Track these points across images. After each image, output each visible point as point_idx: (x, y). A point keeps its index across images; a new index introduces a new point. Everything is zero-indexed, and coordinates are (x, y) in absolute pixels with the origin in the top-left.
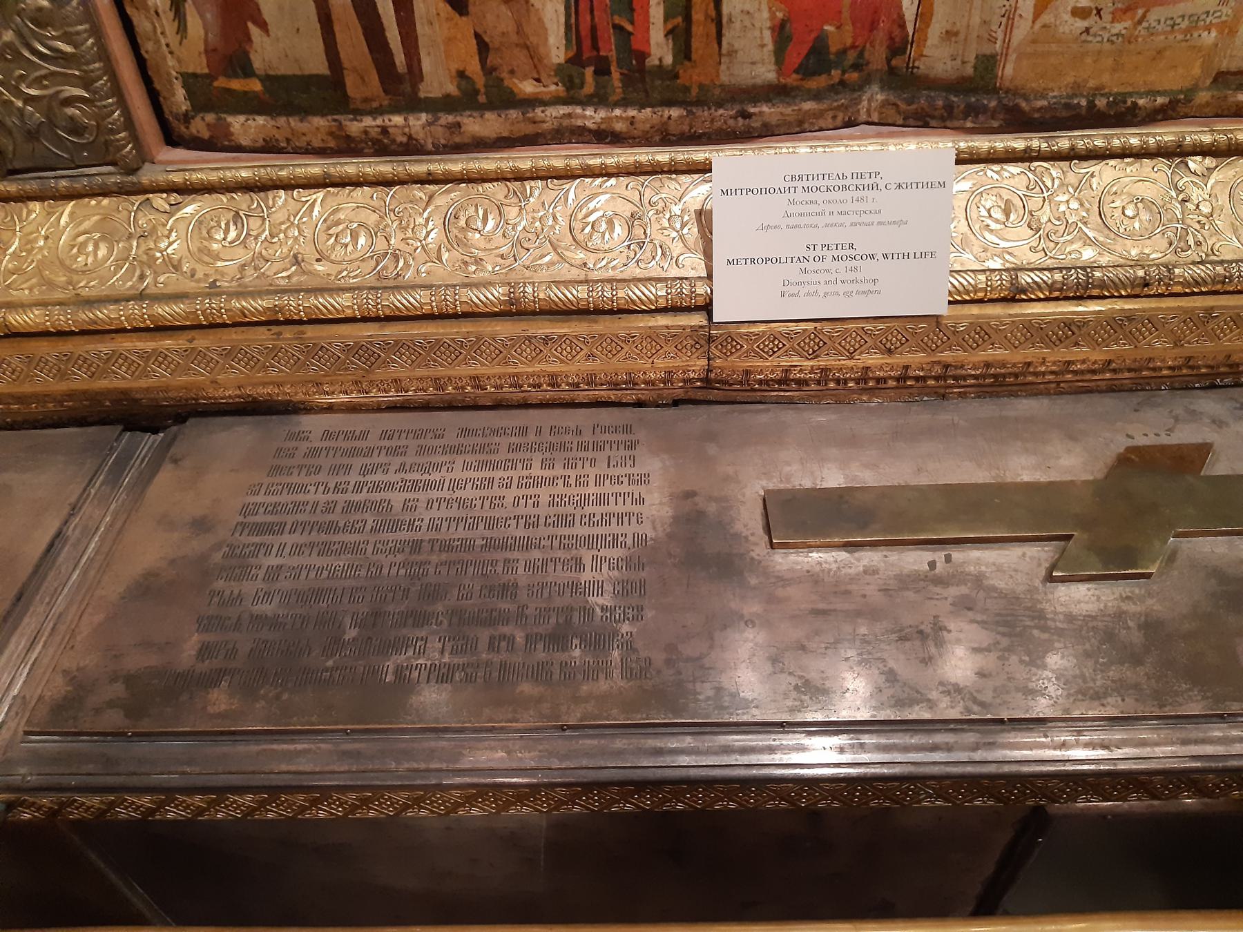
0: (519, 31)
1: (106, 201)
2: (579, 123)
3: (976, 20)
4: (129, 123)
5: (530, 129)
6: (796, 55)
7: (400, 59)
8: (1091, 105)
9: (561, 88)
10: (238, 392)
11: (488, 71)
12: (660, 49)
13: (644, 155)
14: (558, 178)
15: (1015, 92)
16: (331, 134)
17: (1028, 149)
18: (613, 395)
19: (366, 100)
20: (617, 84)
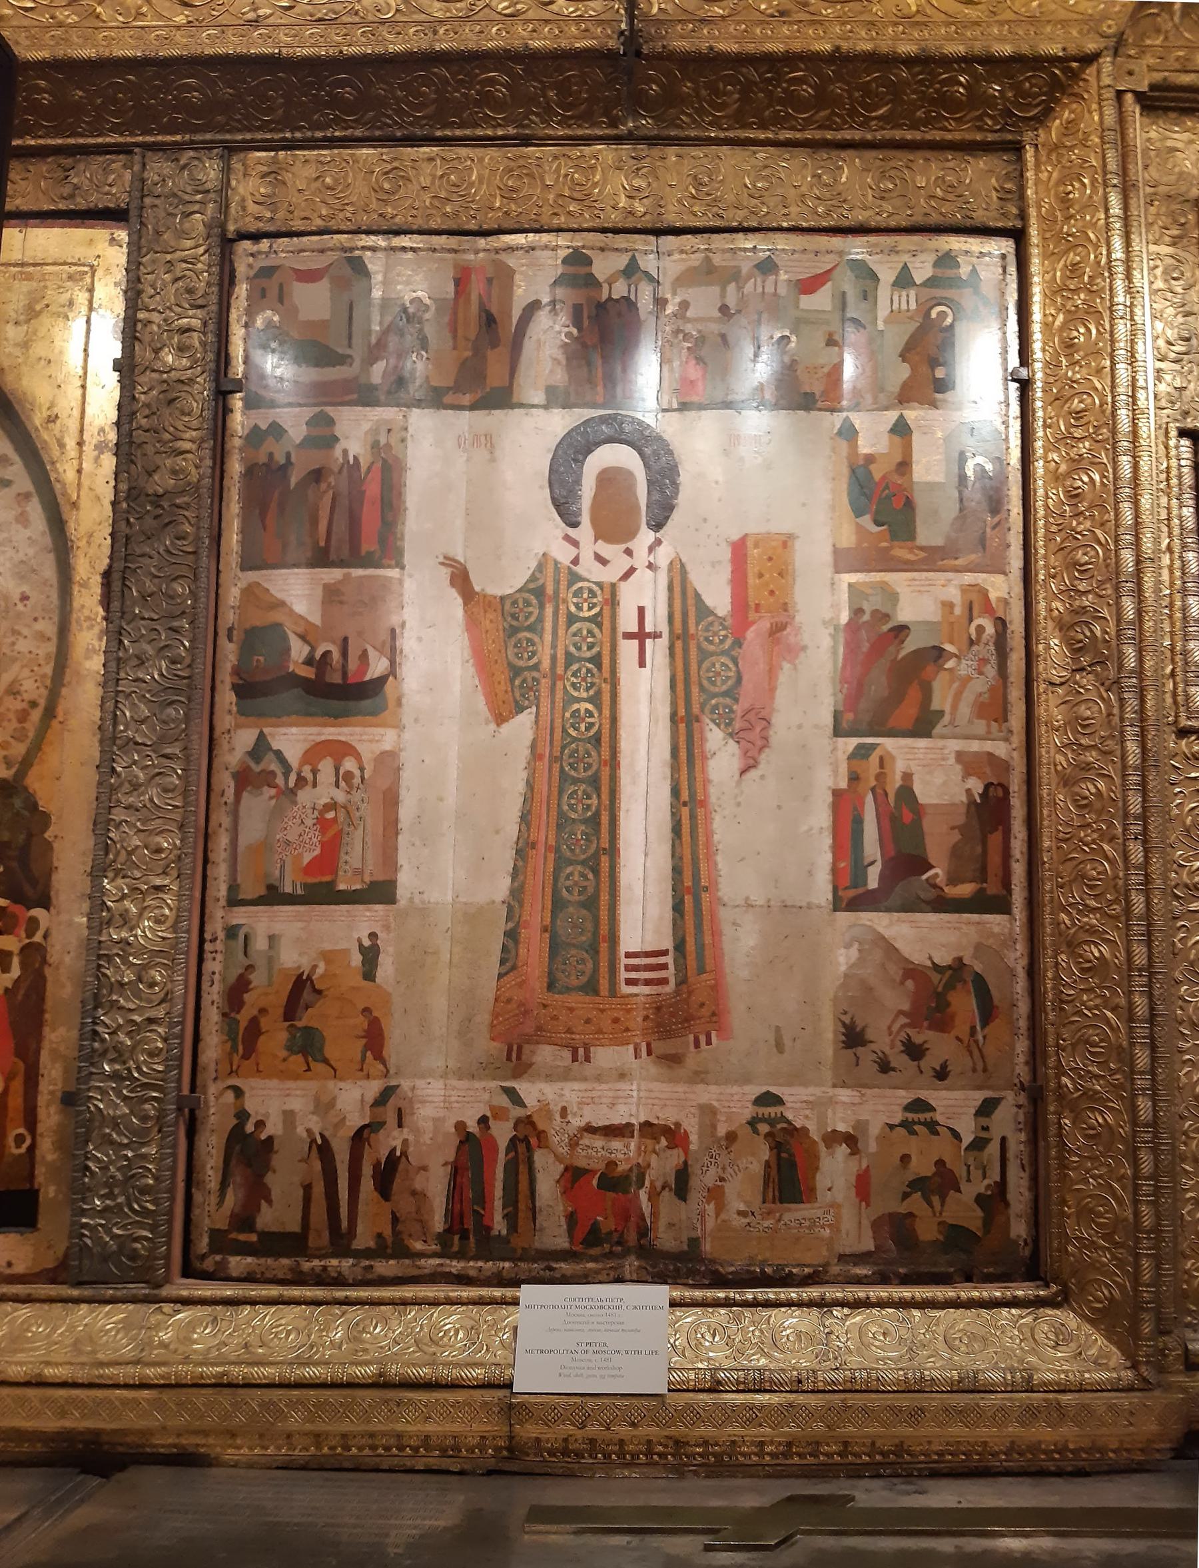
0: (418, 1211)
1: (131, 1307)
2: (447, 1270)
3: (684, 1217)
4: (168, 1257)
5: (416, 1272)
6: (580, 1234)
7: (345, 1224)
8: (763, 1272)
9: (439, 1247)
10: (177, 1441)
11: (396, 1233)
12: (499, 1225)
13: (485, 1292)
14: (429, 1304)
15: (713, 1261)
16: (291, 1270)
17: (727, 1298)
18: (446, 1463)
19: (319, 1249)
20: (473, 1245)
